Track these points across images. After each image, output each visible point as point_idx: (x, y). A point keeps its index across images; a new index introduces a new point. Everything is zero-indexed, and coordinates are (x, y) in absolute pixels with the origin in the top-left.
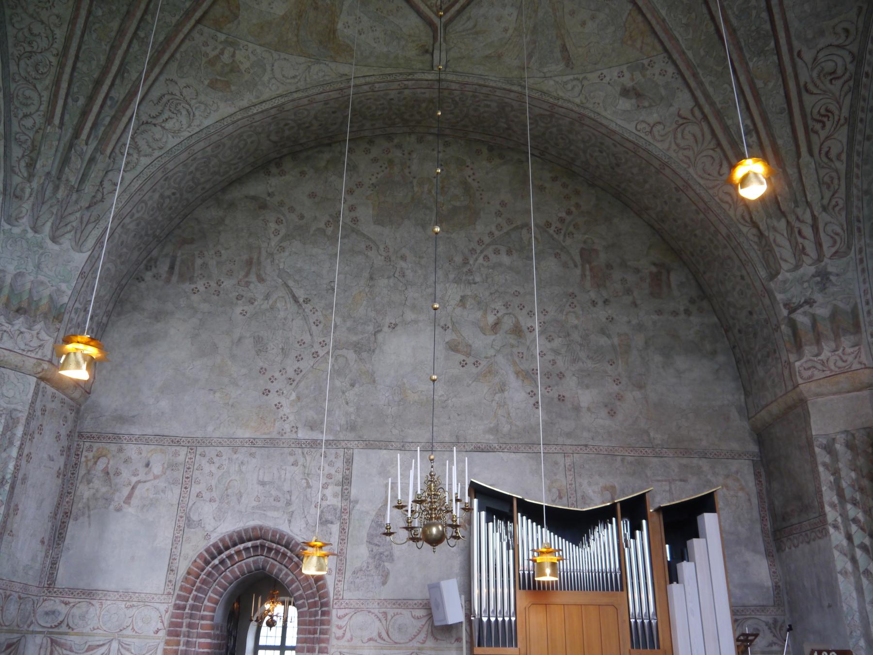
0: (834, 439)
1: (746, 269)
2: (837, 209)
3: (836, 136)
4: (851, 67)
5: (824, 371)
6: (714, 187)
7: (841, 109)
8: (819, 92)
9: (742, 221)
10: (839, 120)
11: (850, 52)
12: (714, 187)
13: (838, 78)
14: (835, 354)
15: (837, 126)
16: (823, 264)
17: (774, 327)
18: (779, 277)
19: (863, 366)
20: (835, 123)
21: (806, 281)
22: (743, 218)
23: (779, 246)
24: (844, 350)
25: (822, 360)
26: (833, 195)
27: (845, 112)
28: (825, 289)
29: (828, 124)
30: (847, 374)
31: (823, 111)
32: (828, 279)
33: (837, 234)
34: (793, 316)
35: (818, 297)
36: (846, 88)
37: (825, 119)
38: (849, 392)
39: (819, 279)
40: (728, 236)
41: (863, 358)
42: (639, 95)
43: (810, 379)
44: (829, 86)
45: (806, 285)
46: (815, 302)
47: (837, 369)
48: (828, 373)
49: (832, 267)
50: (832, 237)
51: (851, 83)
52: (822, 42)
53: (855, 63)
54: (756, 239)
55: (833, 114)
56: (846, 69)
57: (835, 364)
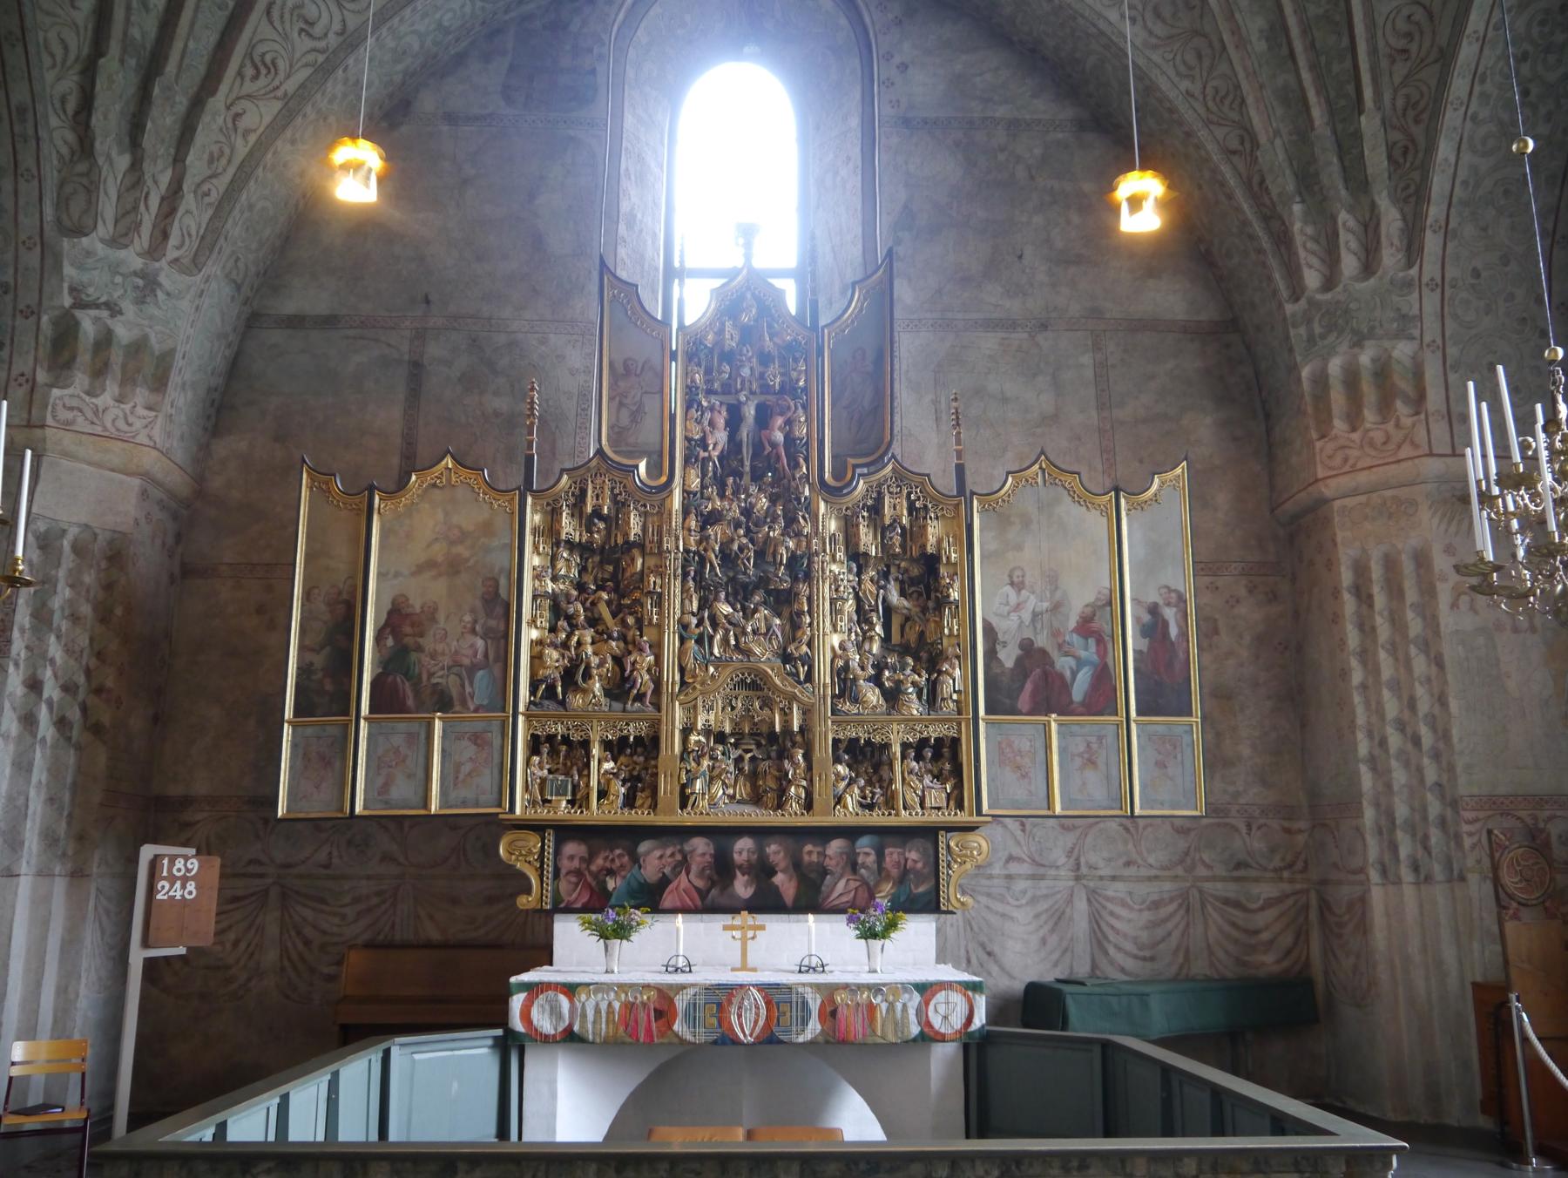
0: (64, 531)
1: (16, 182)
2: (207, 199)
3: (261, 103)
4: (333, 40)
5: (93, 423)
6: (48, 13)
7: (288, 77)
8: (280, 29)
9: (58, 105)
10: (278, 88)
11: (344, 21)
12: (48, 13)
13: (310, 35)
14: (119, 407)
15: (271, 91)
16: (157, 265)
17: (21, 306)
18: (84, 240)
19: (152, 444)
20: (271, 87)
21: (121, 274)
22: (63, 100)
23: (106, 193)
24: (134, 407)
25: (96, 406)
26: (210, 177)
27: (290, 86)
28: (143, 303)
29: (262, 81)
30: (126, 445)
31: (268, 58)
32: (153, 291)
33: (190, 235)
34: (78, 314)
35: (128, 307)
36: (310, 58)
37: (263, 71)
38: (113, 470)
39: (141, 282)
40: (22, 111)
41: (157, 432)
43: (67, 426)
44: (296, 35)
45: (118, 279)
46: (120, 313)
47: (113, 430)
48: (98, 430)
49: (168, 278)
50: (183, 235)
51: (321, 58)
53: (341, 39)
54: (65, 151)
55: (276, 73)
56: (326, 35)
57: (114, 421)
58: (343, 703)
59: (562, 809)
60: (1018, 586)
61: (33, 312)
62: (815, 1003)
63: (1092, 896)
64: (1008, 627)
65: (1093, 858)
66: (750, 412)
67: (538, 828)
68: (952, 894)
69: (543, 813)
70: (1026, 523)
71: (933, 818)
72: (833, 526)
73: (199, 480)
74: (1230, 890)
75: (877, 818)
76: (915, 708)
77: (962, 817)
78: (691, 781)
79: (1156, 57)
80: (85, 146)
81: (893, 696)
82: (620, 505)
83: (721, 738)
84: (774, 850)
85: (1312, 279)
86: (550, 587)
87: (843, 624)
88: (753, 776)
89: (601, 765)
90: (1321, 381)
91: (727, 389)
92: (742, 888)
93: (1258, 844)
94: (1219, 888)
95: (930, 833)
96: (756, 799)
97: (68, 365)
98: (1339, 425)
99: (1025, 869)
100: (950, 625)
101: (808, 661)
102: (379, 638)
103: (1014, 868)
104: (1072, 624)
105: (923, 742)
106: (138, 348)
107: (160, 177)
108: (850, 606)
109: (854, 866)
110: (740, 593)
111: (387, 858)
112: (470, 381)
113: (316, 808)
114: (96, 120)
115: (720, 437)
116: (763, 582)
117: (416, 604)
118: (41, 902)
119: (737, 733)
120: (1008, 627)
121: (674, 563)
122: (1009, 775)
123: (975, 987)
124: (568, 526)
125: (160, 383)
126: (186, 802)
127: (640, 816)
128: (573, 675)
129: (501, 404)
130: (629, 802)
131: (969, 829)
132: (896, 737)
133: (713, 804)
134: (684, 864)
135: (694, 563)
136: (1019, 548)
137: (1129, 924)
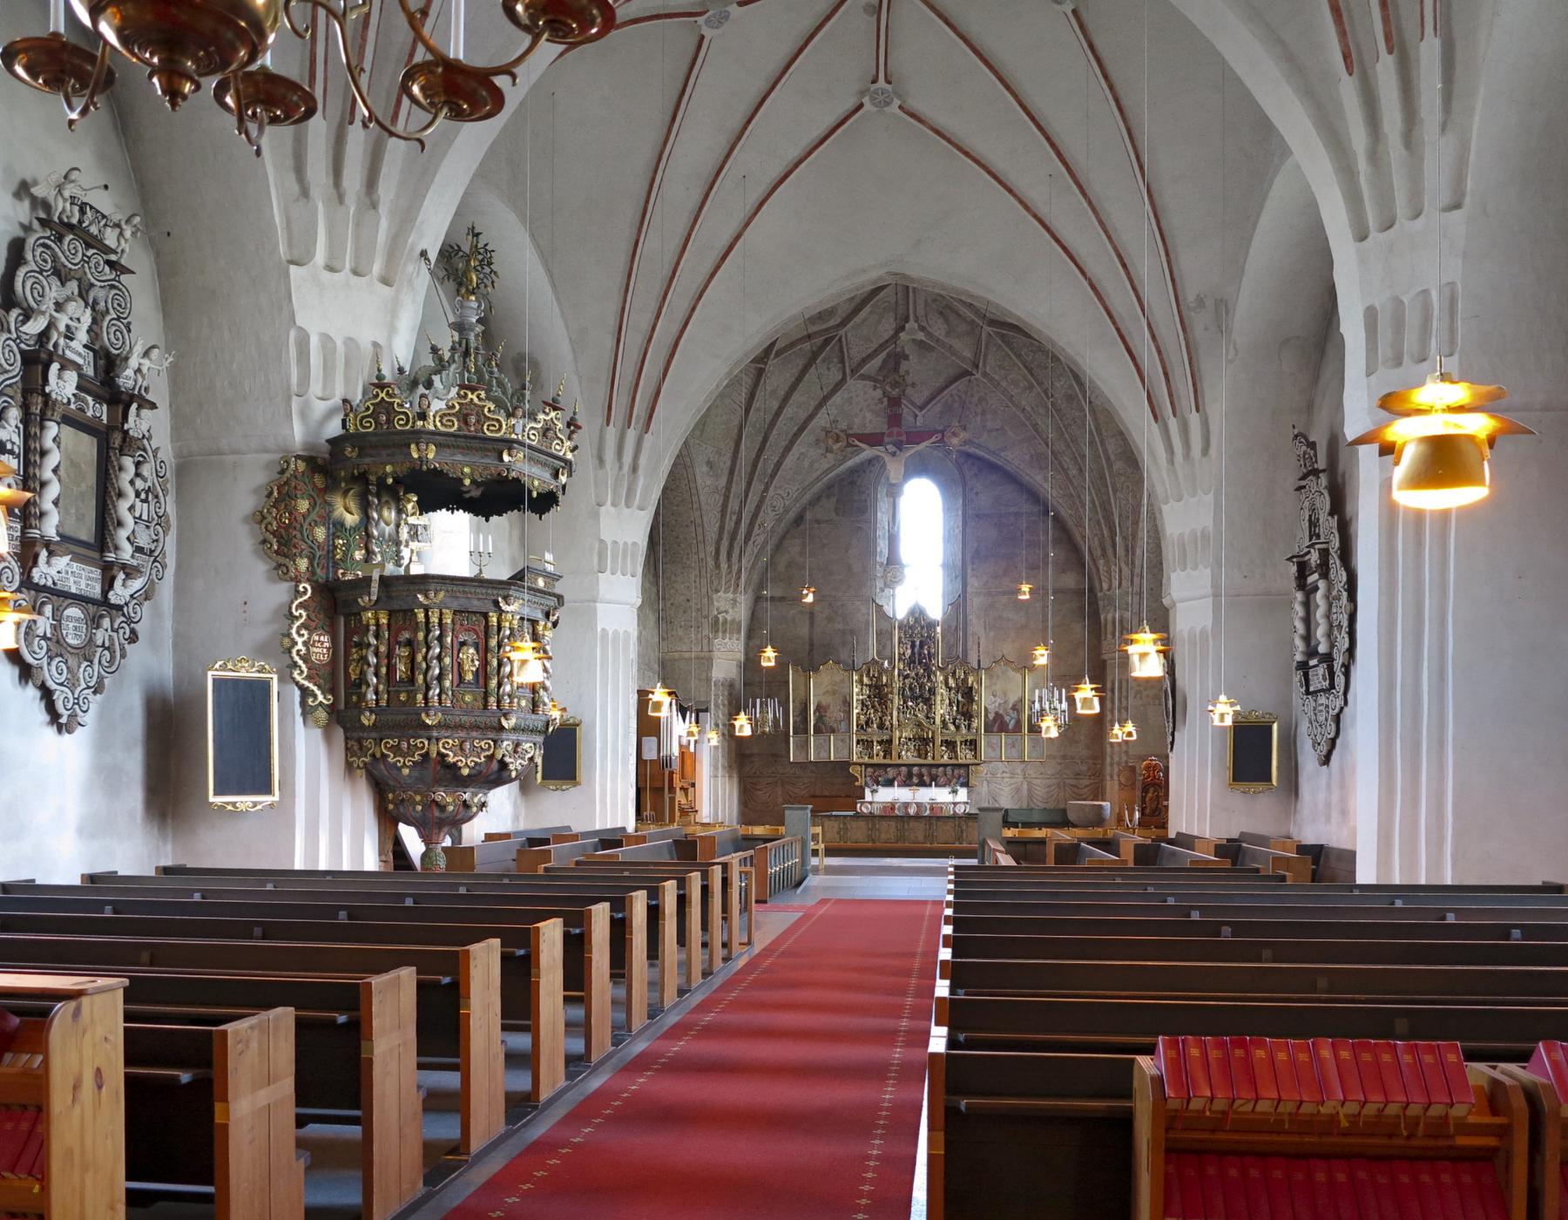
4: (781, 510)
35: (730, 611)
42: (711, 468)
52: (779, 492)
58: (806, 731)
59: (866, 760)
60: (994, 696)
61: (706, 617)
62: (928, 807)
63: (1029, 783)
64: (991, 708)
65: (1030, 772)
66: (918, 643)
67: (860, 765)
68: (972, 781)
69: (861, 761)
70: (998, 677)
71: (968, 762)
72: (941, 678)
73: (746, 654)
74: (1073, 782)
75: (953, 761)
76: (964, 731)
77: (976, 761)
78: (901, 751)
79: (1061, 501)
80: (718, 566)
81: (958, 728)
82: (880, 674)
83: (910, 739)
84: (924, 770)
85: (1105, 586)
86: (861, 697)
87: (944, 707)
88: (919, 750)
89: (877, 748)
90: (1106, 620)
91: (911, 636)
92: (915, 780)
93: (1084, 768)
94: (1070, 781)
95: (967, 766)
96: (919, 756)
97: (717, 631)
98: (1109, 636)
99: (1008, 775)
100: (975, 707)
101: (934, 718)
102: (814, 713)
103: (1004, 775)
104: (1010, 706)
105: (966, 741)
106: (733, 621)
107: (735, 568)
108: (947, 701)
109: (945, 775)
110: (914, 699)
111: (812, 772)
112: (830, 619)
113: (801, 759)
114: (721, 558)
115: (909, 651)
116: (921, 696)
117: (824, 703)
118: (724, 784)
119: (915, 739)
120: (991, 708)
121: (896, 691)
122: (990, 750)
123: (967, 803)
124: (866, 680)
125: (739, 632)
126: (751, 755)
127: (887, 761)
128: (868, 722)
129: (840, 626)
130: (885, 757)
131: (979, 764)
132: (958, 739)
133: (907, 757)
134: (899, 774)
135: (902, 690)
136: (995, 684)
137: (1040, 791)
